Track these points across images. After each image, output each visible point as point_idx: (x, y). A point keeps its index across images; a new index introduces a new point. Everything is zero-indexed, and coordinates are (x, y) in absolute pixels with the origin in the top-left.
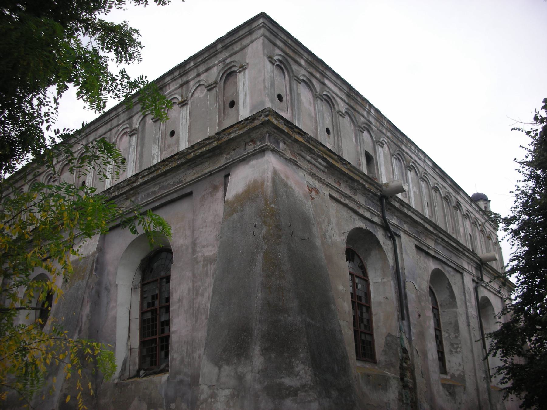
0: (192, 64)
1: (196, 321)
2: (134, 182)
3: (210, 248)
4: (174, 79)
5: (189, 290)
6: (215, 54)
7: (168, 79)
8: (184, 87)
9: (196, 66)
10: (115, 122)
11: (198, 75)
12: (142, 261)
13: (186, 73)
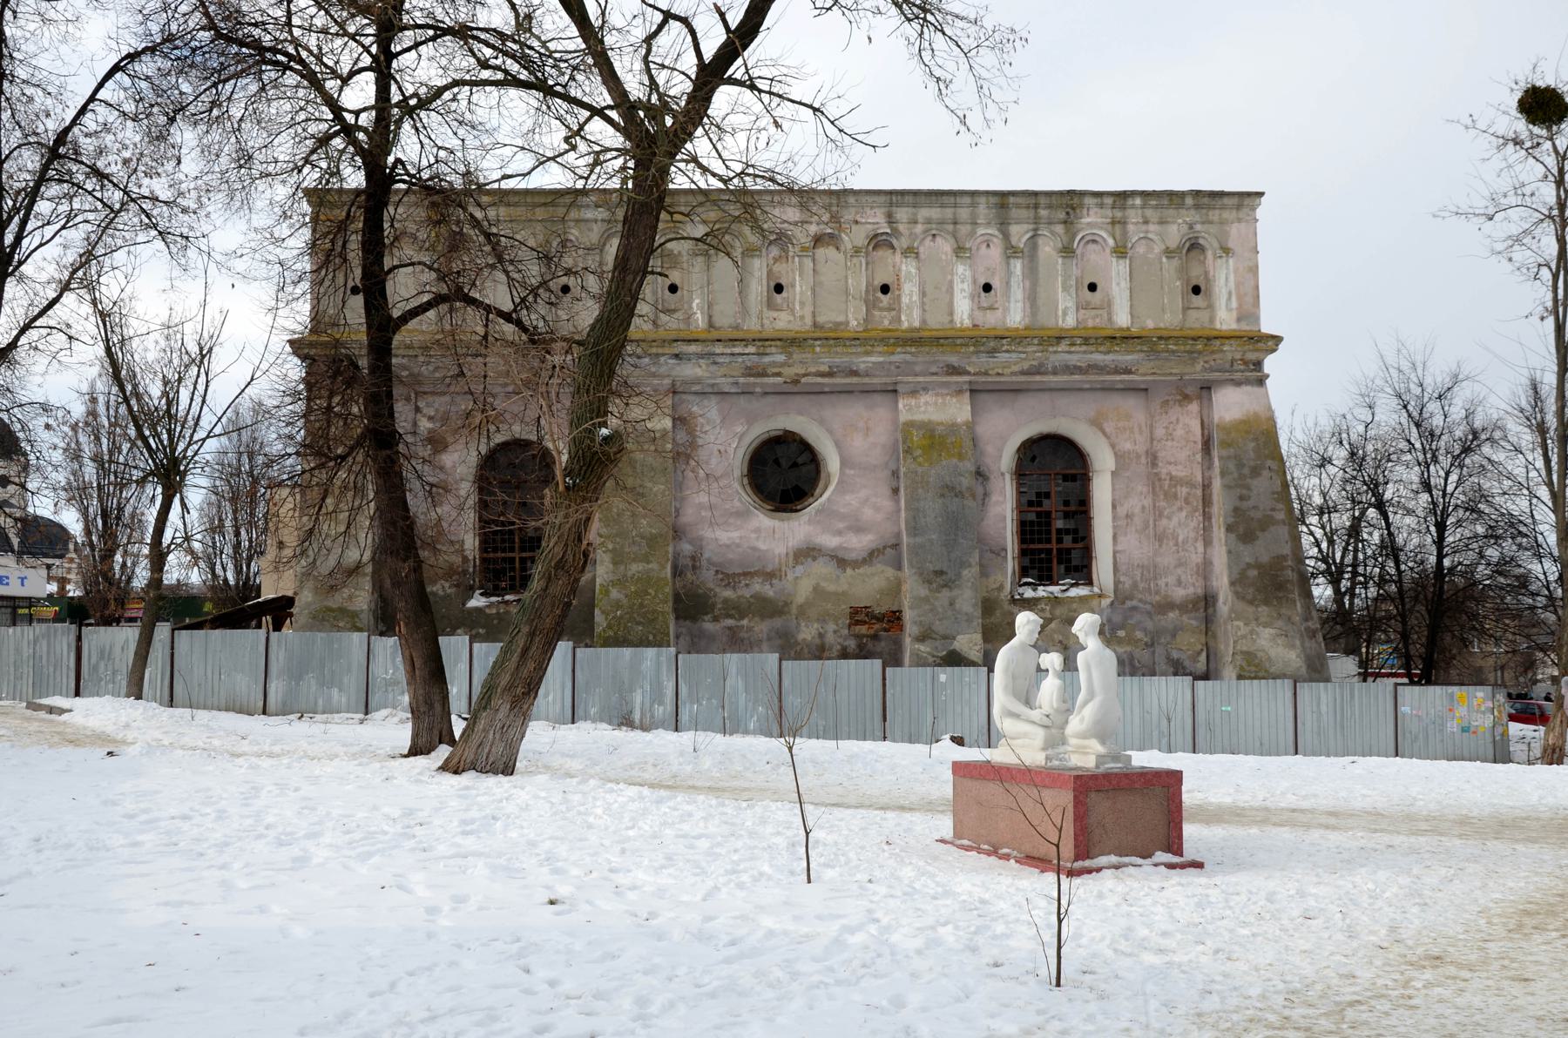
0: (1138, 201)
1: (1160, 546)
3: (1180, 467)
4: (1101, 206)
5: (1143, 508)
6: (1181, 205)
7: (1088, 201)
8: (1117, 227)
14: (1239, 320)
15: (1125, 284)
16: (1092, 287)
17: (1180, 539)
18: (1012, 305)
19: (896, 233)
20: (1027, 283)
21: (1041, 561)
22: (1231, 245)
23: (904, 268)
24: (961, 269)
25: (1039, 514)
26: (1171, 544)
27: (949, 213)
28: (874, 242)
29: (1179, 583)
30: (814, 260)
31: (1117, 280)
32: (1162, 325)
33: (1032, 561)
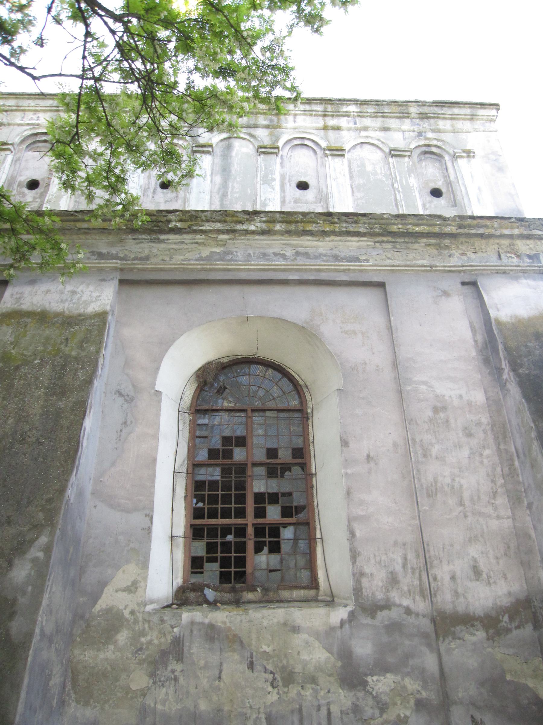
2: (241, 222)
9: (360, 115)
12: (210, 363)
17: (466, 495)
21: (226, 546)
25: (226, 471)
26: (452, 501)
28: (30, 141)
29: (477, 572)
33: (211, 548)
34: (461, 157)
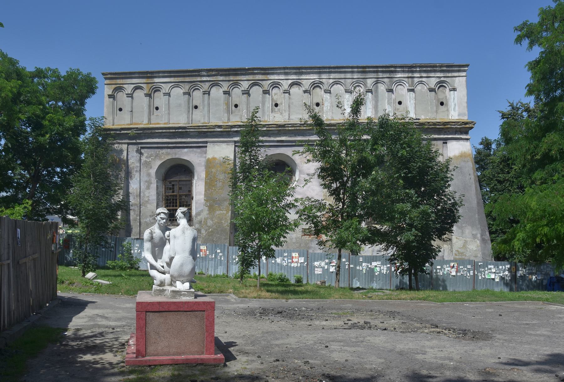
6: (435, 71)
8: (410, 79)
9: (420, 72)
10: (349, 76)
11: (421, 77)
13: (413, 72)
14: (459, 115)
15: (413, 102)
16: (400, 103)
18: (368, 110)
19: (321, 83)
20: (374, 102)
22: (456, 86)
23: (325, 96)
24: (347, 96)
27: (342, 76)
30: (290, 94)
31: (410, 101)
32: (428, 118)
34: (452, 91)
